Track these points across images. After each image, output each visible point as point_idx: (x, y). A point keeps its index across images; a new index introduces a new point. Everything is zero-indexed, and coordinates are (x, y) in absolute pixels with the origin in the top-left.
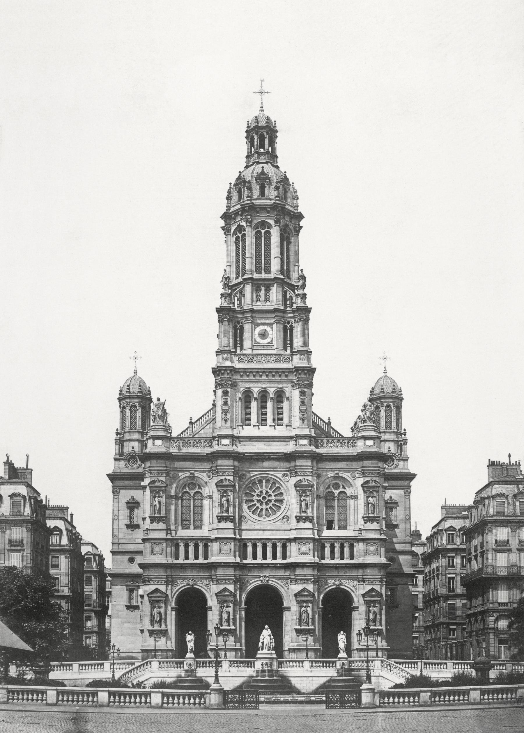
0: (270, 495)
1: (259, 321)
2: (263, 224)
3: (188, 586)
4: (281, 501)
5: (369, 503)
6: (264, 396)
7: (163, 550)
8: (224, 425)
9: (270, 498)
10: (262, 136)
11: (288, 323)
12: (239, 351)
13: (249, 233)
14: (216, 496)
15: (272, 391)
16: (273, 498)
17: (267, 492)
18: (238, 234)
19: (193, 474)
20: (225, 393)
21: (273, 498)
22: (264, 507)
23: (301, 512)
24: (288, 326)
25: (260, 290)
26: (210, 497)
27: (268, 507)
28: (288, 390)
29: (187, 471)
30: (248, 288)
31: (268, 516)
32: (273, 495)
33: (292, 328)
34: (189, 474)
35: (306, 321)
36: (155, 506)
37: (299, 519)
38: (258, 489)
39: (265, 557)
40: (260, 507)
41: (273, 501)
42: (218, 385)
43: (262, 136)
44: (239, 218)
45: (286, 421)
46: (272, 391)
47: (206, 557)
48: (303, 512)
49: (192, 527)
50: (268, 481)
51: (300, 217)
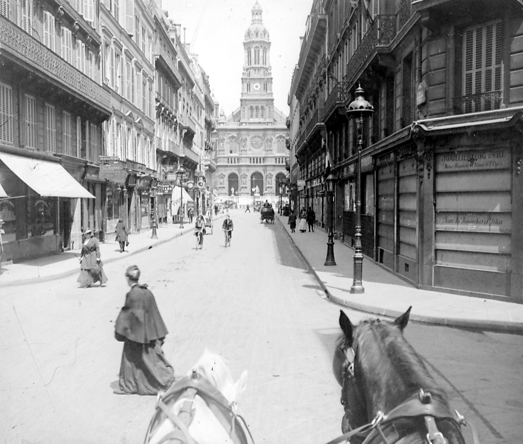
2: (257, 47)
15: (260, 106)
21: (260, 143)
43: (257, 12)
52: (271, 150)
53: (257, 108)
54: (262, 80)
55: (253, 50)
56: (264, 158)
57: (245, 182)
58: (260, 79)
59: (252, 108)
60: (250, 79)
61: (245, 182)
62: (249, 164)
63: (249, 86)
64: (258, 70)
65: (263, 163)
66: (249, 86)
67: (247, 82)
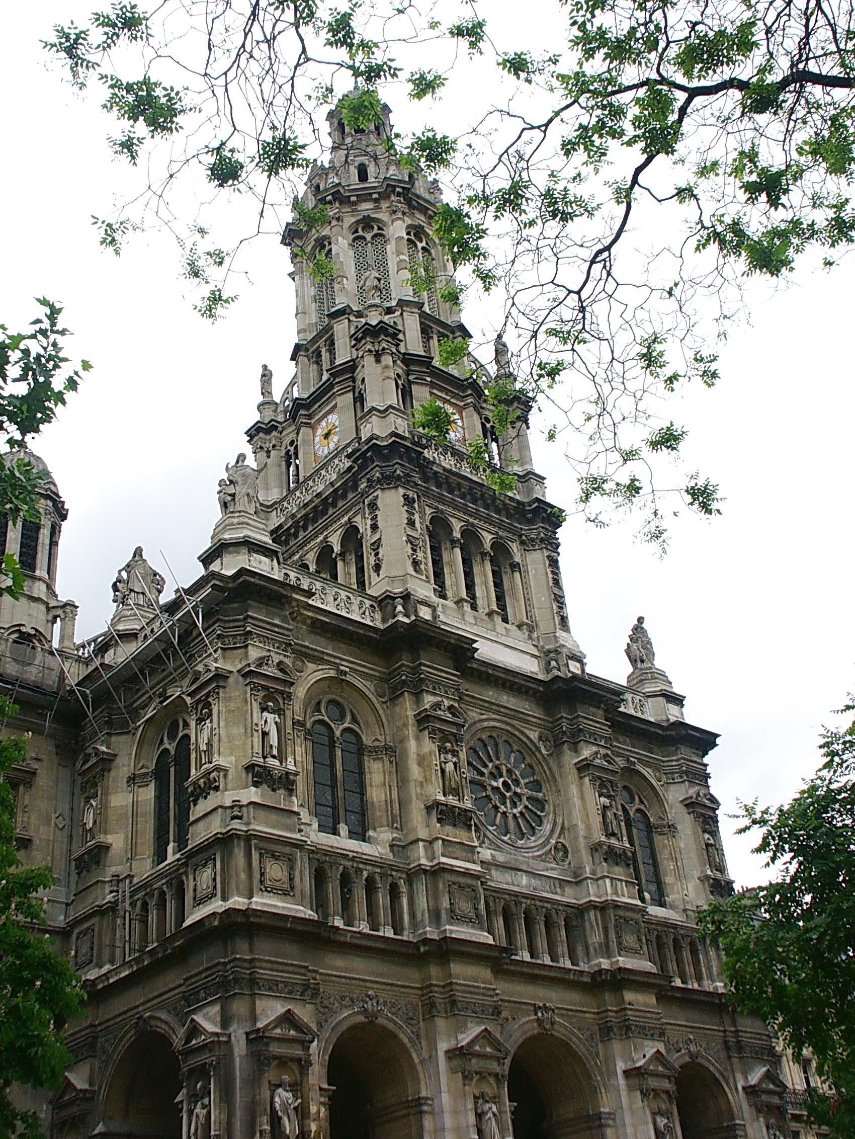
0: (517, 782)
1: (435, 391)
3: (361, 1018)
4: (541, 804)
5: (707, 845)
7: (291, 879)
8: (411, 570)
9: (518, 790)
11: (488, 421)
13: (398, 229)
14: (419, 747)
15: (487, 538)
17: (509, 771)
18: (361, 233)
19: (345, 673)
20: (408, 501)
24: (488, 425)
25: (429, 338)
27: (515, 811)
29: (329, 662)
32: (522, 782)
34: (332, 673)
36: (265, 734)
38: (491, 761)
40: (502, 808)
41: (524, 799)
44: (366, 206)
48: (613, 834)
49: (343, 829)
60: (408, 360)
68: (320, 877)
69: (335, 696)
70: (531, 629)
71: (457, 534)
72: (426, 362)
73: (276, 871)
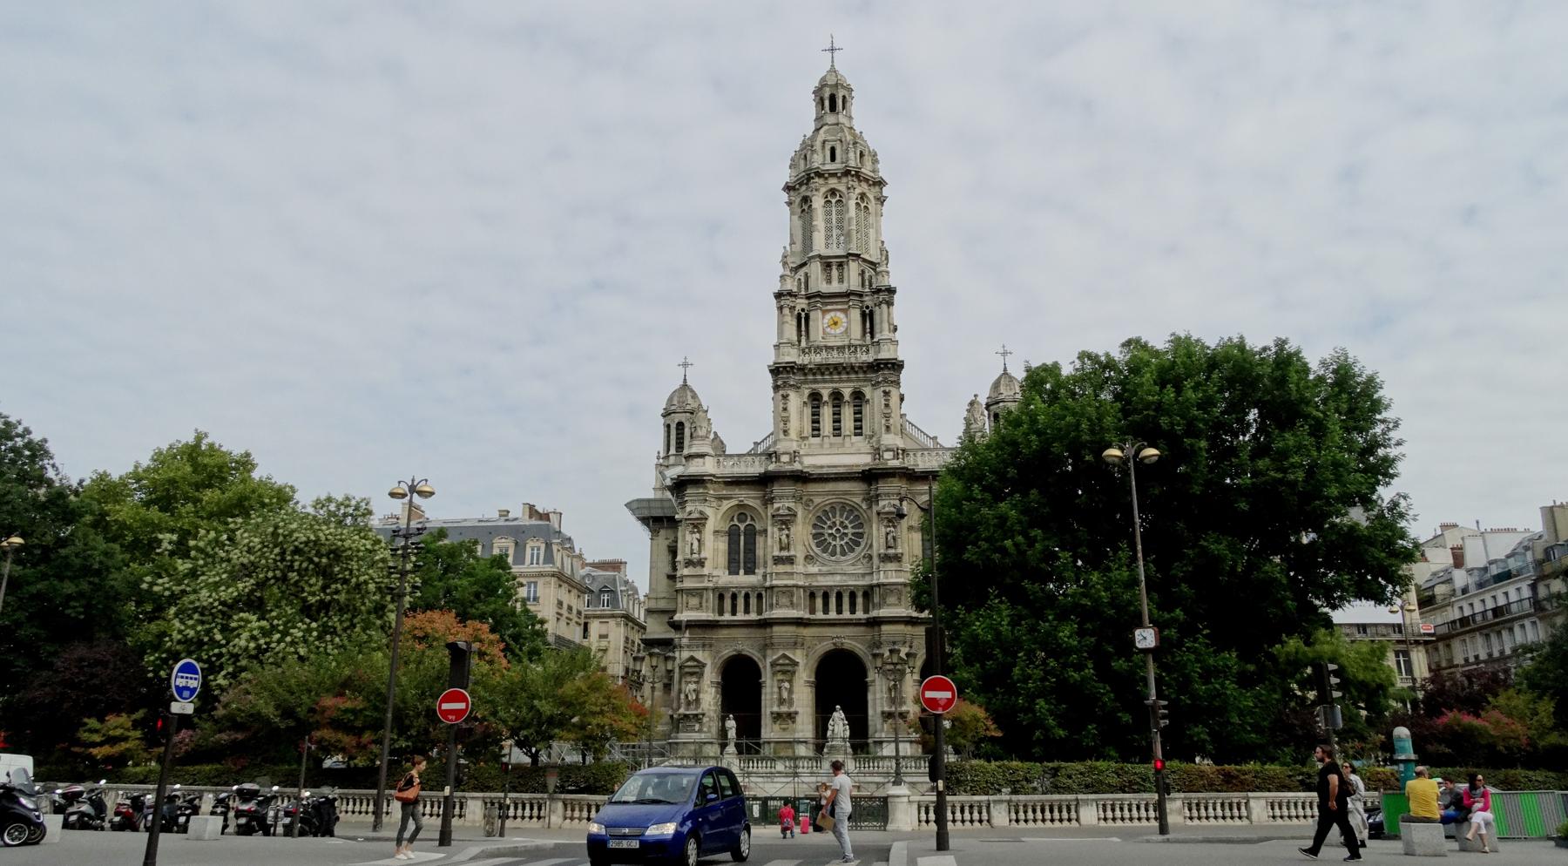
2: (833, 192)
4: (861, 535)
6: (837, 396)
10: (832, 99)
12: (803, 344)
14: (773, 531)
15: (847, 392)
16: (850, 531)
21: (850, 531)
22: (838, 542)
23: (889, 548)
26: (765, 531)
28: (867, 391)
30: (815, 269)
31: (843, 553)
33: (872, 313)
35: (890, 304)
37: (886, 558)
39: (839, 611)
42: (776, 388)
43: (832, 99)
45: (866, 430)
46: (847, 392)
47: (760, 612)
50: (843, 508)
51: (880, 183)
52: (897, 558)
53: (837, 396)
54: (854, 300)
55: (818, 202)
56: (868, 592)
57: (792, 695)
58: (847, 295)
59: (815, 397)
61: (792, 695)
62: (803, 613)
63: (803, 321)
64: (840, 265)
65: (866, 611)
66: (803, 321)
67: (799, 306)
68: (721, 597)
69: (742, 511)
70: (871, 437)
71: (826, 398)
72: (819, 295)
73: (694, 601)
